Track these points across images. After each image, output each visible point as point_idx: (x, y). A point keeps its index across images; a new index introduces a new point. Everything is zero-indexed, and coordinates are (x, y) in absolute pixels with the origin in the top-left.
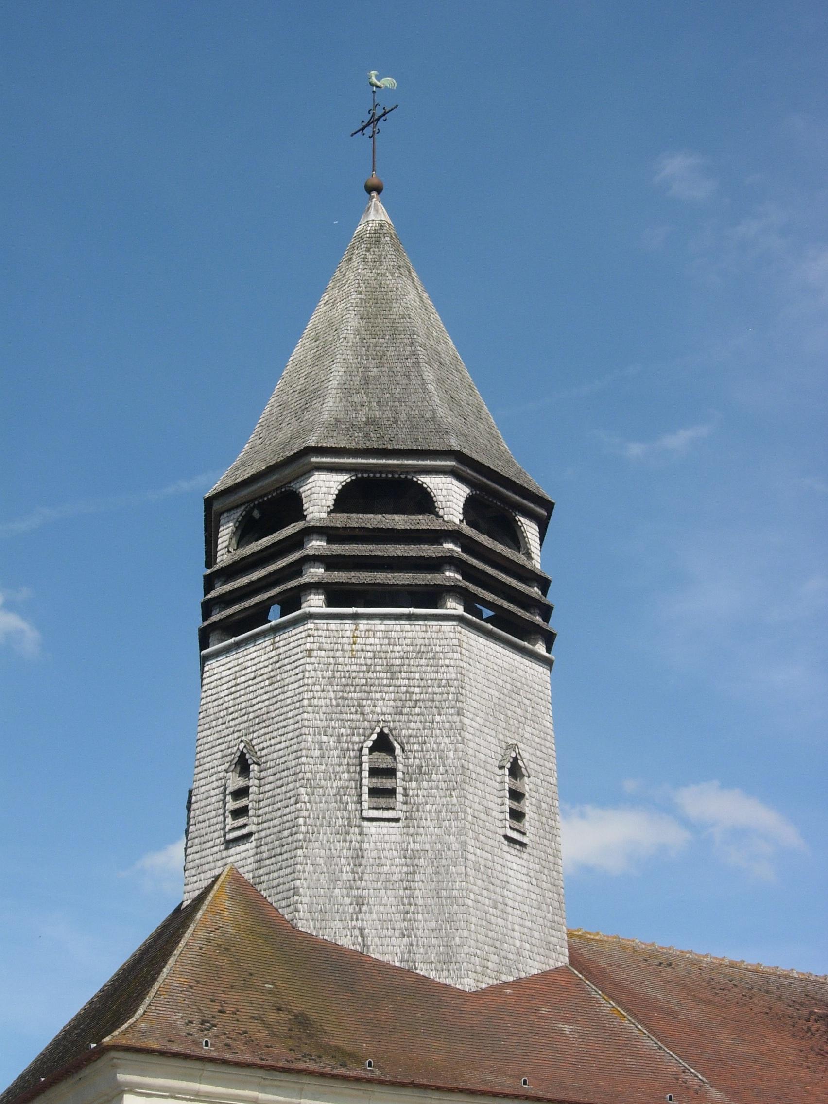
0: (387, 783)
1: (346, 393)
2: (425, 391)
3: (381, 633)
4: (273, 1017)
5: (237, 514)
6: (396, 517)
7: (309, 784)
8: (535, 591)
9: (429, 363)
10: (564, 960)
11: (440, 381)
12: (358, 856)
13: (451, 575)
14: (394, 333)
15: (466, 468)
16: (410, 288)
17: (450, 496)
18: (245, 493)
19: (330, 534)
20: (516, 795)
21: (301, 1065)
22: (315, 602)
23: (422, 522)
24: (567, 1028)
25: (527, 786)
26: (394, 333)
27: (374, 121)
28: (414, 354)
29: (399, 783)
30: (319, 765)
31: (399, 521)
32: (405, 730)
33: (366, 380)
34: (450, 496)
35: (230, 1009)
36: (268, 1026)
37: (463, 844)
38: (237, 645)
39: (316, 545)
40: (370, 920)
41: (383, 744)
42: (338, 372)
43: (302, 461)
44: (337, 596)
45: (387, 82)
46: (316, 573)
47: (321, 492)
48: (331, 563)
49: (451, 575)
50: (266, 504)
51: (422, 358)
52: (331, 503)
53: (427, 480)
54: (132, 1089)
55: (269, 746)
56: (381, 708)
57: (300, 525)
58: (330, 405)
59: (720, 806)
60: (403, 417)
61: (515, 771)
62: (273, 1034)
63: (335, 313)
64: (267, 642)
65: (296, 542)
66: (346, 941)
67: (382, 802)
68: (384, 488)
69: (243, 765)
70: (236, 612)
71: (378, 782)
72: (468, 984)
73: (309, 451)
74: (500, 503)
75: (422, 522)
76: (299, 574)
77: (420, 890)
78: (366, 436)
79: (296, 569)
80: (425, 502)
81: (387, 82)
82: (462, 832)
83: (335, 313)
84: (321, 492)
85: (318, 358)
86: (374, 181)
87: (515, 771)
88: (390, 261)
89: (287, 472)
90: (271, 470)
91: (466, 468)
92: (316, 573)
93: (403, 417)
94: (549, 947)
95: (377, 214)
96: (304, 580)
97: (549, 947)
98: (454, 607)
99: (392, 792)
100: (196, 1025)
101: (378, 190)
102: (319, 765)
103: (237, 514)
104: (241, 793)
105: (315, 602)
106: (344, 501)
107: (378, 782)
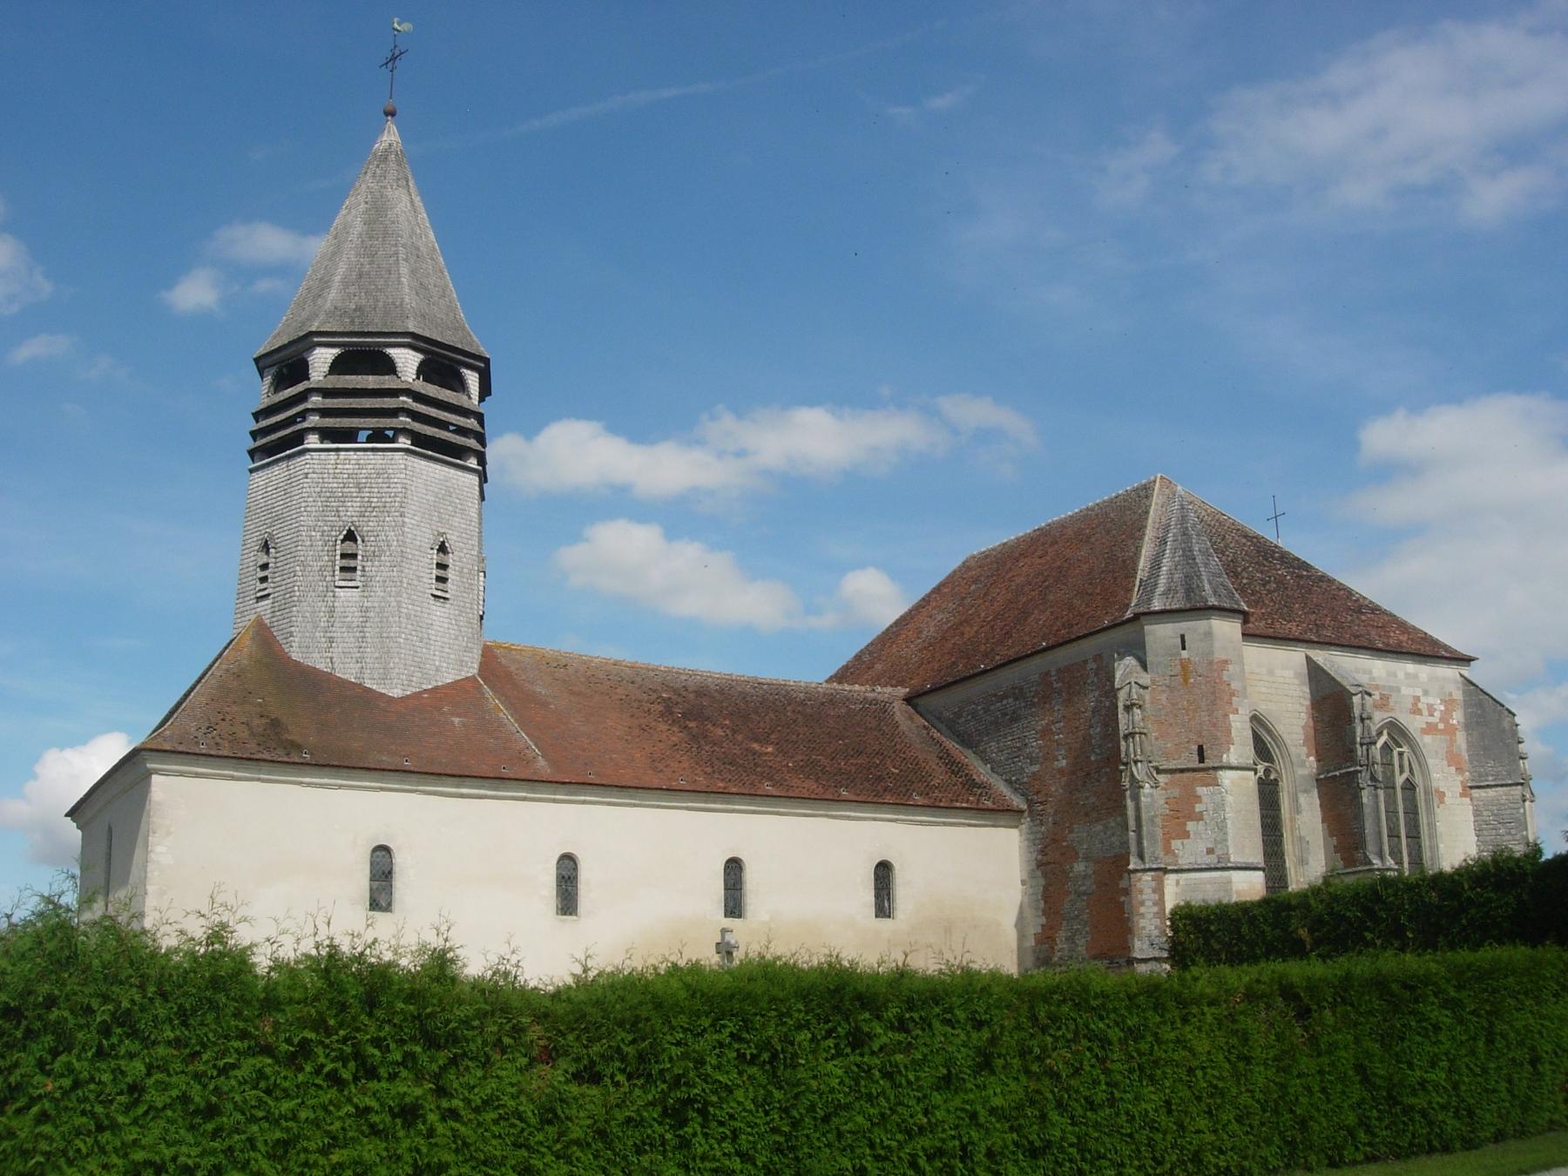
0: (352, 563)
1: (346, 283)
2: (400, 282)
3: (355, 461)
4: (256, 722)
5: (273, 370)
6: (371, 378)
7: (303, 565)
8: (471, 423)
9: (406, 260)
10: (472, 669)
11: (413, 272)
12: (332, 611)
13: (404, 420)
14: (386, 234)
15: (416, 342)
16: (405, 198)
17: (407, 361)
18: (277, 357)
19: (327, 393)
20: (442, 566)
21: (259, 756)
22: (312, 441)
23: (387, 382)
24: (456, 720)
25: (450, 560)
26: (386, 234)
27: (393, 59)
28: (396, 253)
29: (358, 563)
30: (312, 550)
31: (371, 381)
32: (367, 527)
33: (360, 276)
34: (407, 361)
35: (228, 718)
36: (250, 728)
37: (399, 603)
38: (268, 465)
39: (316, 401)
40: (336, 651)
41: (350, 536)
42: (342, 269)
43: (307, 341)
44: (327, 434)
45: (406, 27)
46: (314, 420)
47: (321, 359)
48: (325, 412)
49: (404, 420)
50: (286, 366)
51: (401, 256)
52: (326, 369)
53: (391, 351)
54: (157, 772)
55: (282, 536)
56: (351, 514)
57: (300, 387)
58: (333, 295)
59: (973, 412)
60: (381, 304)
61: (442, 549)
62: (253, 734)
63: (349, 218)
64: (283, 465)
65: (303, 397)
66: (322, 666)
67: (348, 575)
68: (364, 356)
69: (266, 547)
70: (275, 441)
71: (346, 563)
72: (396, 692)
73: (312, 334)
74: (443, 364)
75: (387, 382)
76: (304, 419)
77: (370, 632)
78: (352, 322)
79: (303, 415)
80: (389, 367)
81: (406, 27)
82: (399, 594)
83: (349, 218)
84: (321, 359)
85: (334, 254)
86: (390, 108)
87: (442, 549)
88: (392, 174)
89: (300, 346)
90: (291, 343)
91: (416, 342)
92: (314, 420)
93: (381, 304)
94: (462, 663)
95: (390, 136)
96: (306, 425)
97: (462, 663)
98: (403, 442)
99: (354, 569)
100: (203, 730)
101: (392, 114)
102: (312, 550)
103: (273, 370)
104: (265, 567)
105: (312, 441)
106: (337, 367)
107: (346, 563)
